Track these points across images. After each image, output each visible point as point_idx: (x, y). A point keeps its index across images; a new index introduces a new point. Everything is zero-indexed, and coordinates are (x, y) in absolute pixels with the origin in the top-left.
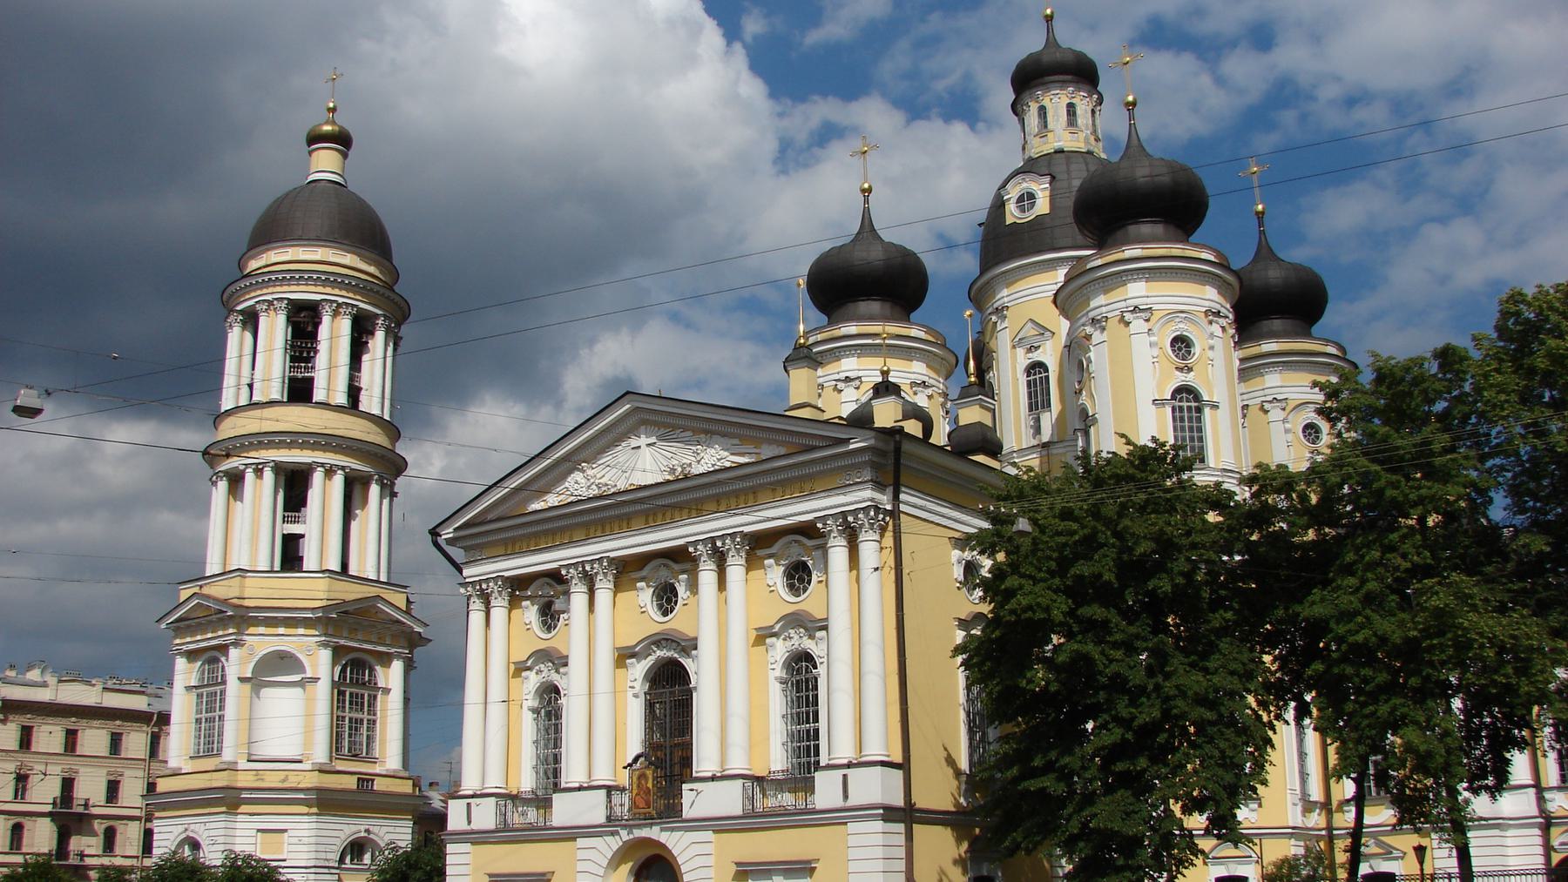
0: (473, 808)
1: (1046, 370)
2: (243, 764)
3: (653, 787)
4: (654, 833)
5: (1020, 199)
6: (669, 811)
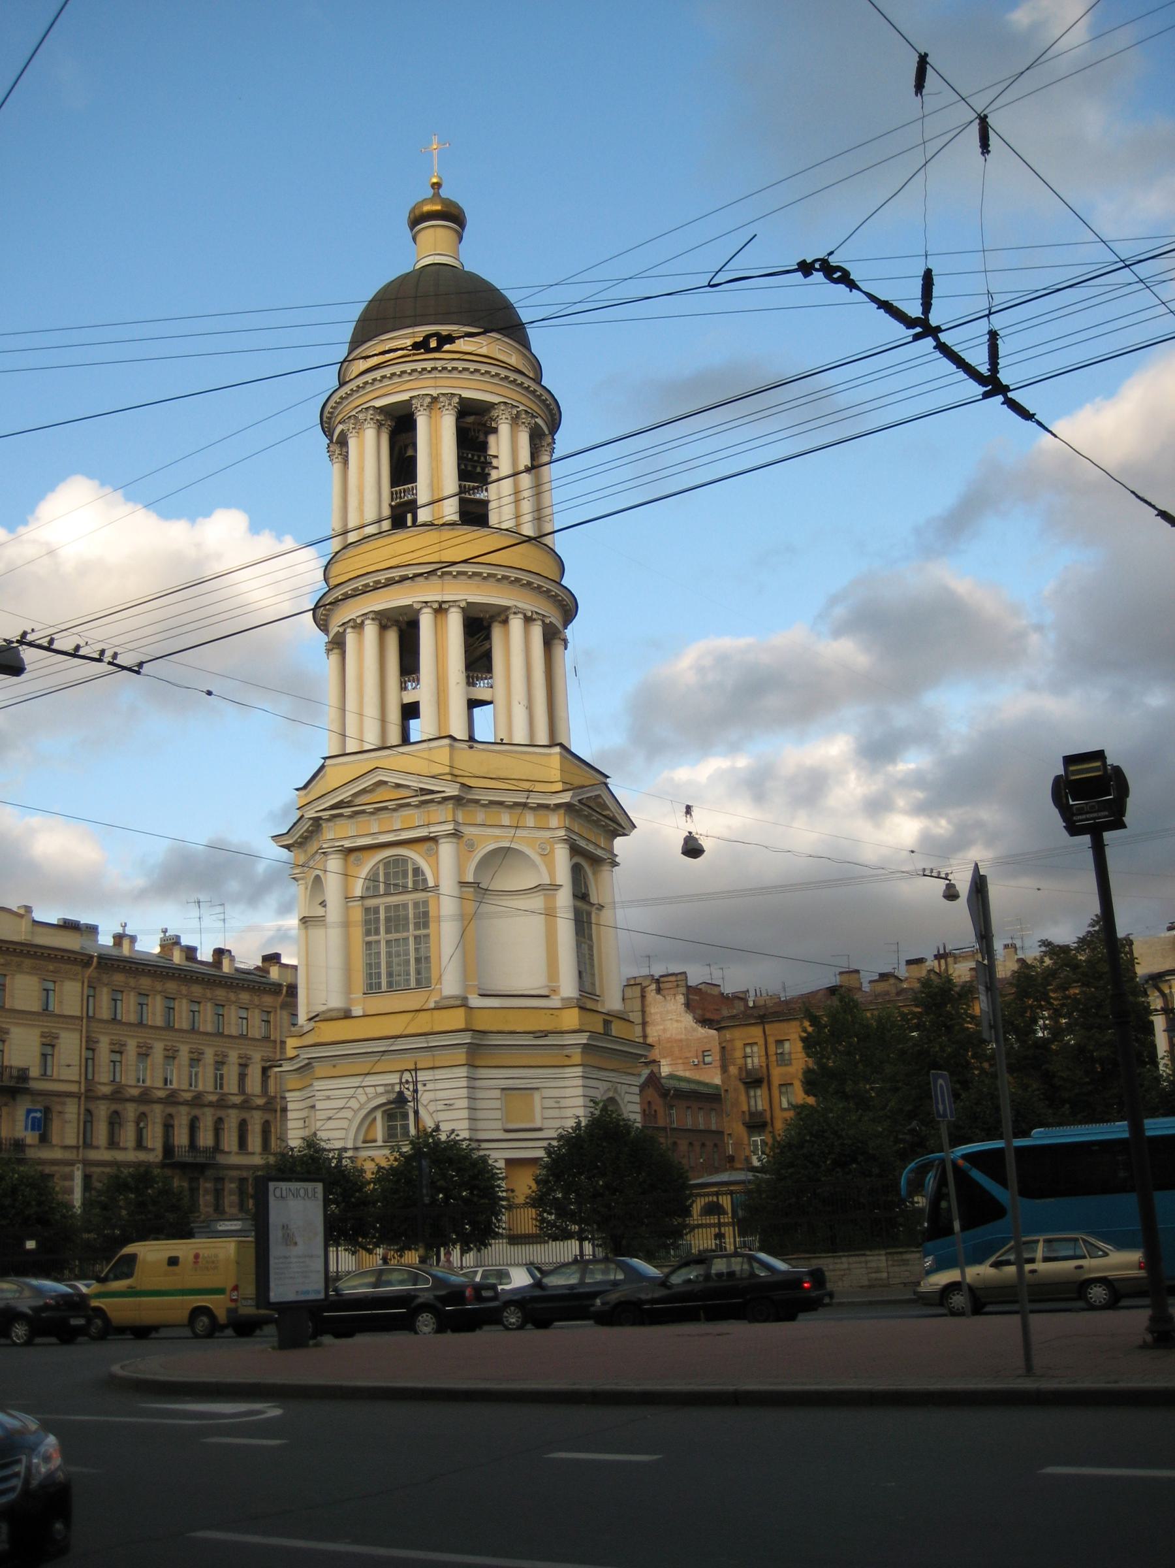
2: (475, 1001)
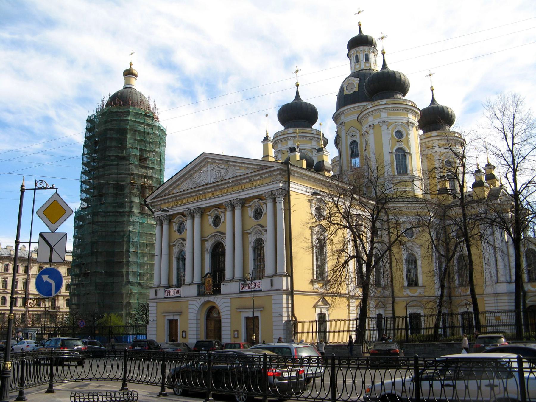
1: (357, 143)
4: (212, 298)
6: (217, 291)
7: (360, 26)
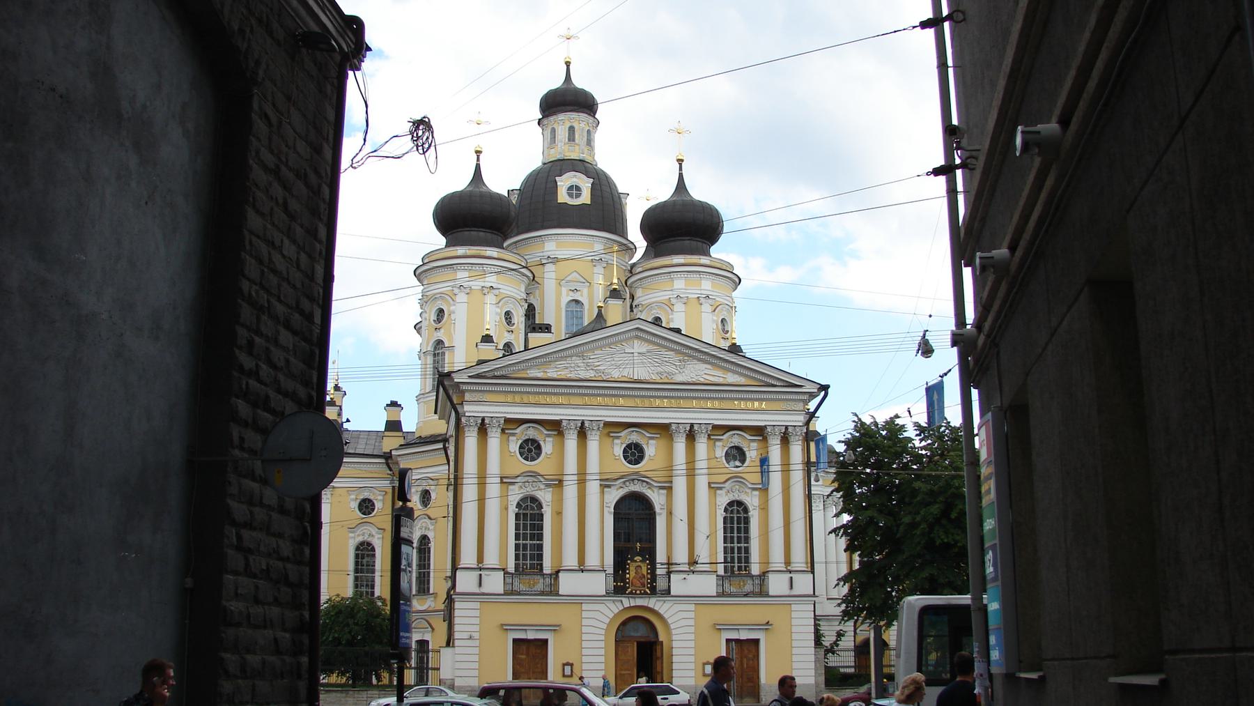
0: (483, 575)
3: (648, 573)
4: (652, 602)
5: (571, 188)
7: (568, 64)
